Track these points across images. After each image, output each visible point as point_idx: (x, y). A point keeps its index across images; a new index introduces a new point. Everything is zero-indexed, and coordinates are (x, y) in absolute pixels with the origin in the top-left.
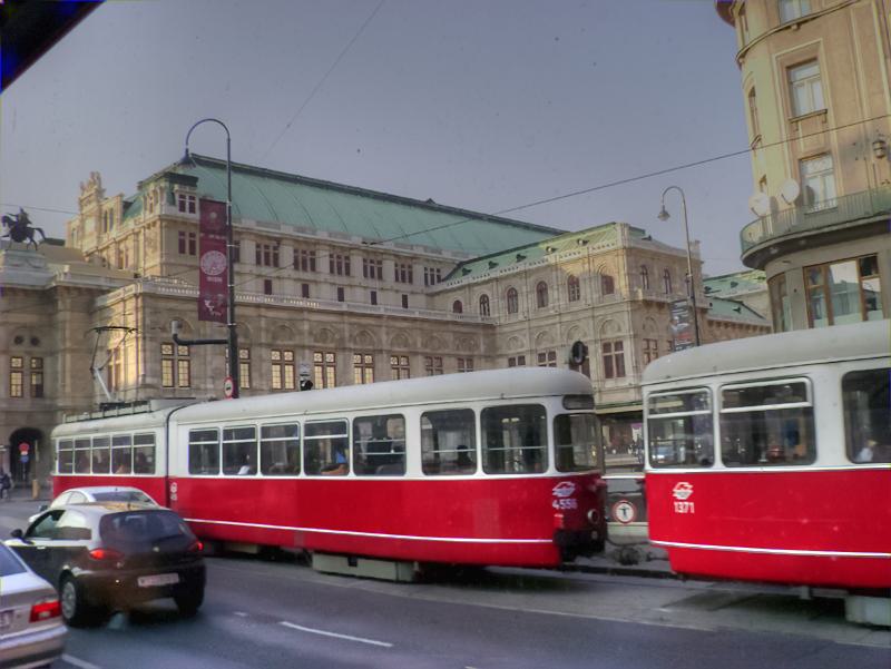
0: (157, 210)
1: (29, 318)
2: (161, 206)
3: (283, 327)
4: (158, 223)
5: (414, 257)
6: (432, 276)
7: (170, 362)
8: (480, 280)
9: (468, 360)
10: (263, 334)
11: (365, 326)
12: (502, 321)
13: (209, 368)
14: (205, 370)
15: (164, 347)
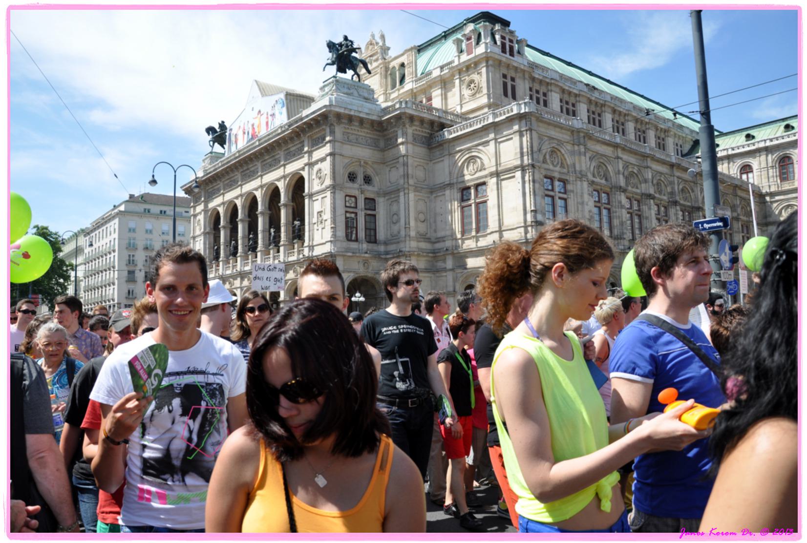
0: (481, 50)
1: (364, 153)
2: (486, 44)
3: (632, 174)
4: (484, 64)
5: (666, 131)
6: (677, 150)
7: (550, 199)
8: (742, 150)
9: (747, 227)
10: (621, 176)
11: (686, 181)
12: (773, 189)
13: (587, 208)
14: (583, 211)
15: (545, 180)
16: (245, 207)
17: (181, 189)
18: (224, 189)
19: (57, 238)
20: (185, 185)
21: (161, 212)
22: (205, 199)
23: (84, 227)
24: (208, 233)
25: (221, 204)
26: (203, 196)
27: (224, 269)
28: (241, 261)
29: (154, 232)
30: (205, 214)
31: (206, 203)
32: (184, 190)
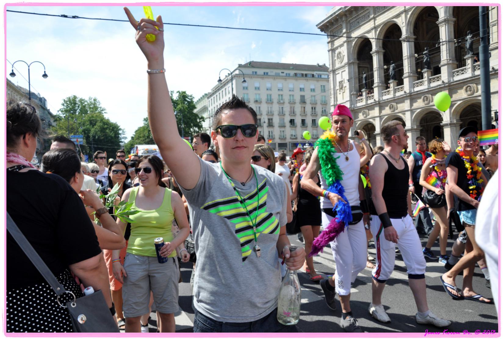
16: (411, 22)
17: (316, 28)
18: (375, 13)
19: (192, 99)
20: (323, 21)
21: (264, 73)
22: (347, 30)
23: (207, 93)
24: (353, 63)
25: (372, 29)
26: (344, 25)
27: (381, 95)
28: (409, 82)
29: (261, 88)
30: (348, 45)
31: (349, 33)
32: (319, 28)
